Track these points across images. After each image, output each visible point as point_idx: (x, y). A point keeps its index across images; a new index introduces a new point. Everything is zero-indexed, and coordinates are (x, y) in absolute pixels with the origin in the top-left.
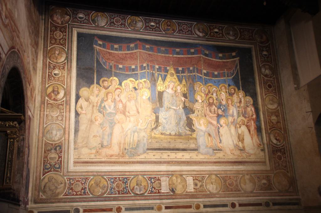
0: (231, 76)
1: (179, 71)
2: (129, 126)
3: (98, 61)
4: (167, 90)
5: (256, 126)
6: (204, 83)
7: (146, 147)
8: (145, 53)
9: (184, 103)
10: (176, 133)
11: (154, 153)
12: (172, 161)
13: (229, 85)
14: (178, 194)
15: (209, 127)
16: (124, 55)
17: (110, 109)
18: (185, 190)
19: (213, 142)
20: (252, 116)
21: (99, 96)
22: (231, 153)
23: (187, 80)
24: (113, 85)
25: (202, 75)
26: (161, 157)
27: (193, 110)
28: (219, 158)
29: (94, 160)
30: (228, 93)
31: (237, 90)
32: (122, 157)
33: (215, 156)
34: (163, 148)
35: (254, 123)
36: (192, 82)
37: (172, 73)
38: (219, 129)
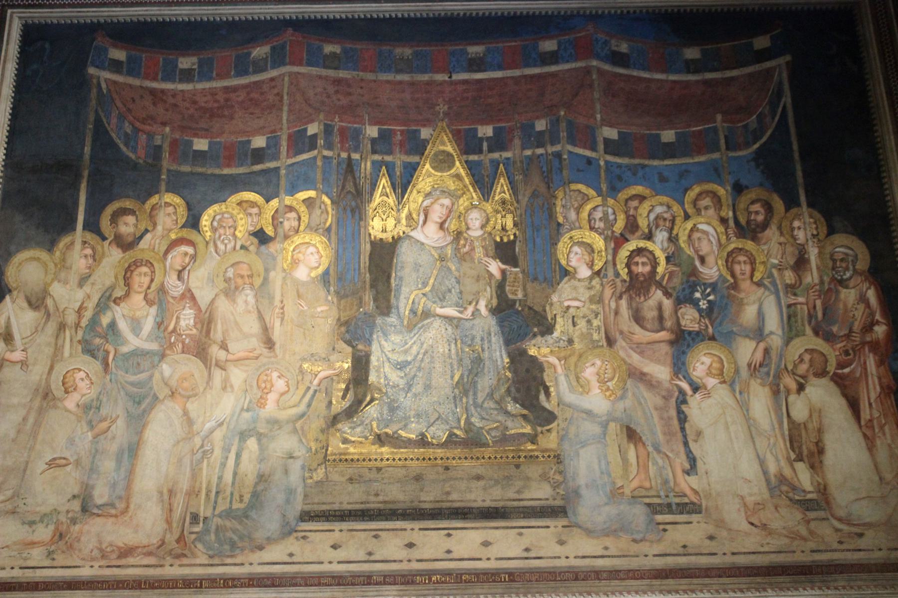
0: (747, 145)
1: (481, 139)
2: (221, 406)
3: (100, 131)
4: (417, 234)
5: (888, 380)
6: (604, 187)
7: (299, 505)
8: (320, 77)
9: (501, 286)
10: (452, 434)
11: (337, 534)
12: (430, 573)
13: (738, 189)
15: (630, 394)
16: (221, 97)
17: (138, 336)
19: (652, 470)
20: (868, 327)
21: (91, 280)
22: (752, 524)
23: (519, 177)
24: (159, 228)
25: (593, 149)
26: (370, 554)
27: (546, 318)
28: (681, 551)
29: (40, 575)
30: (731, 223)
31: (778, 204)
32: (178, 556)
33: (659, 541)
34: (381, 506)
35: (880, 363)
36: (543, 189)
37: (444, 151)
38: (682, 400)
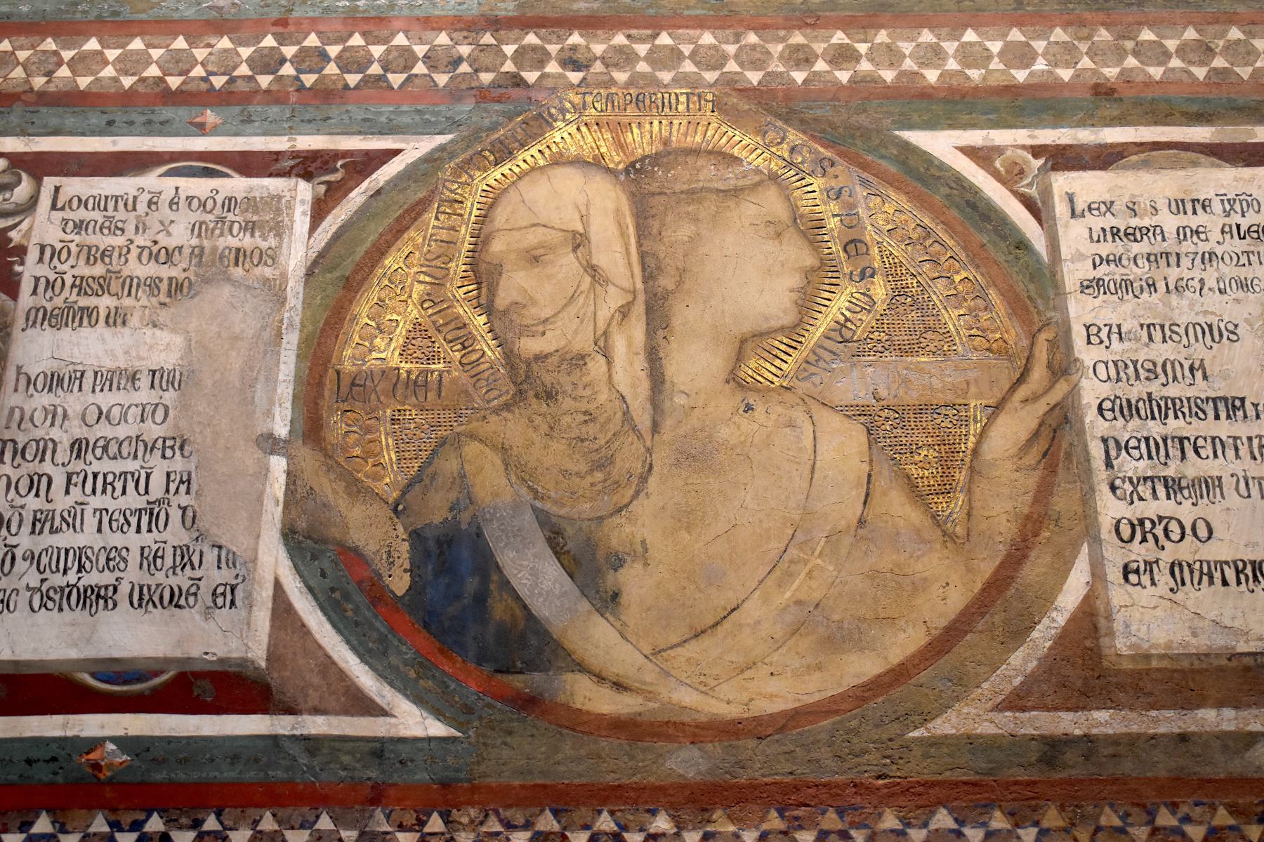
14: (685, 763)
18: (1001, 601)
